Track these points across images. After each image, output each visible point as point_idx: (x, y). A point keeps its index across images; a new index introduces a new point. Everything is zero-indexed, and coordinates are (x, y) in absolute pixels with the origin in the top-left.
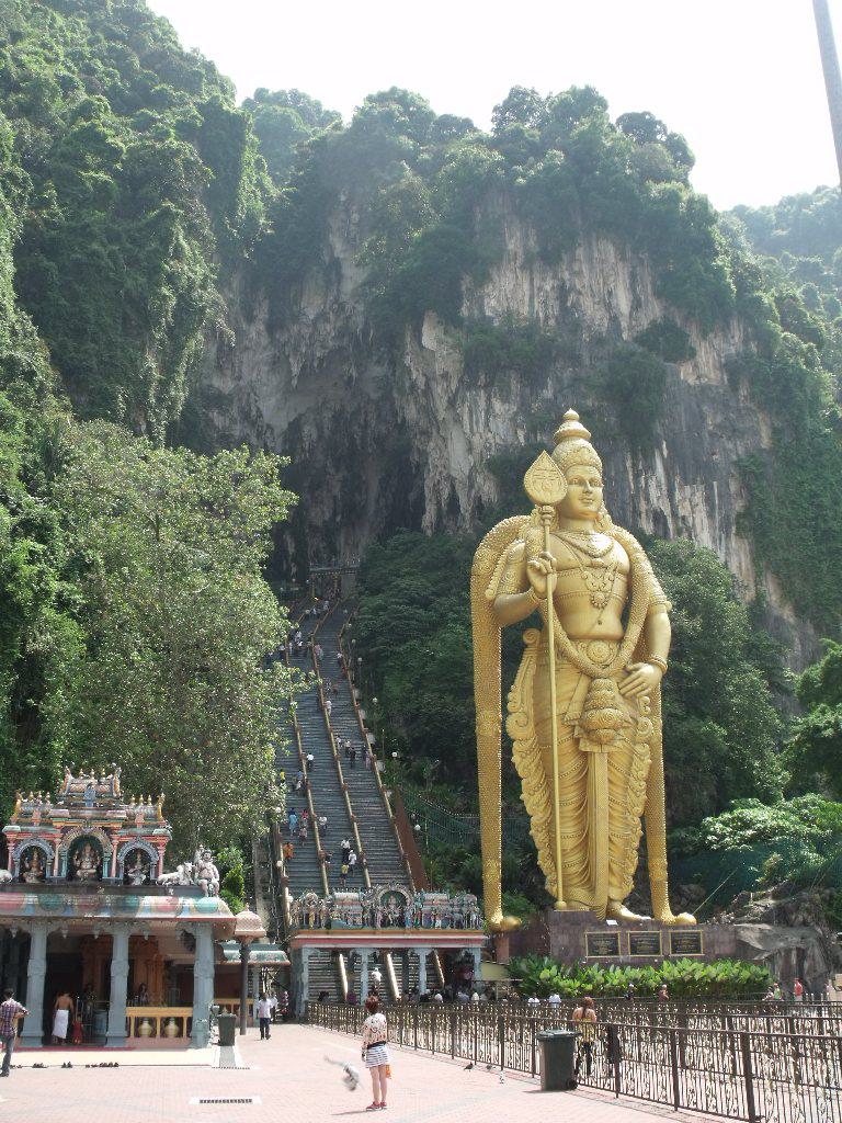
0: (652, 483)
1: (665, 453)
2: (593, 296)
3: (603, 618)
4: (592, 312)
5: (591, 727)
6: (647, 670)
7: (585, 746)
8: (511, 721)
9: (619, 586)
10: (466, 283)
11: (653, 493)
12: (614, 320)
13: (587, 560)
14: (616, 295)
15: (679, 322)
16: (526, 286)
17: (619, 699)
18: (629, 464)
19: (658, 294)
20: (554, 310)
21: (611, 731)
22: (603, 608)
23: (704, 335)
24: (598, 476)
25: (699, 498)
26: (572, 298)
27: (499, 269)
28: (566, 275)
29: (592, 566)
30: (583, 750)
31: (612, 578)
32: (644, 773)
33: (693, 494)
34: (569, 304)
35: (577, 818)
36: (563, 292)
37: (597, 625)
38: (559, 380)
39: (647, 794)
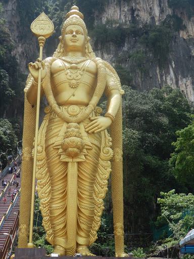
0: (168, 79)
1: (174, 66)
2: (145, 11)
3: (76, 93)
4: (144, 17)
5: (64, 147)
6: (103, 122)
7: (64, 158)
8: (34, 151)
9: (87, 79)
10: (97, 13)
11: (169, 82)
12: (153, 18)
13: (67, 65)
14: (154, 10)
15: (179, 16)
16: (118, 11)
17: (84, 134)
18: (158, 72)
19: (170, 6)
20: (129, 18)
21: (74, 149)
22: (75, 88)
23: (189, 18)
24: (81, 29)
25: (189, 83)
26: (136, 13)
27: (108, 7)
28: (134, 4)
29: (71, 68)
30: (63, 160)
31: (82, 73)
32: (107, 176)
33: (187, 82)
34: (135, 15)
35: (61, 198)
36: (133, 11)
37: (72, 97)
38: (129, 42)
39: (108, 187)
